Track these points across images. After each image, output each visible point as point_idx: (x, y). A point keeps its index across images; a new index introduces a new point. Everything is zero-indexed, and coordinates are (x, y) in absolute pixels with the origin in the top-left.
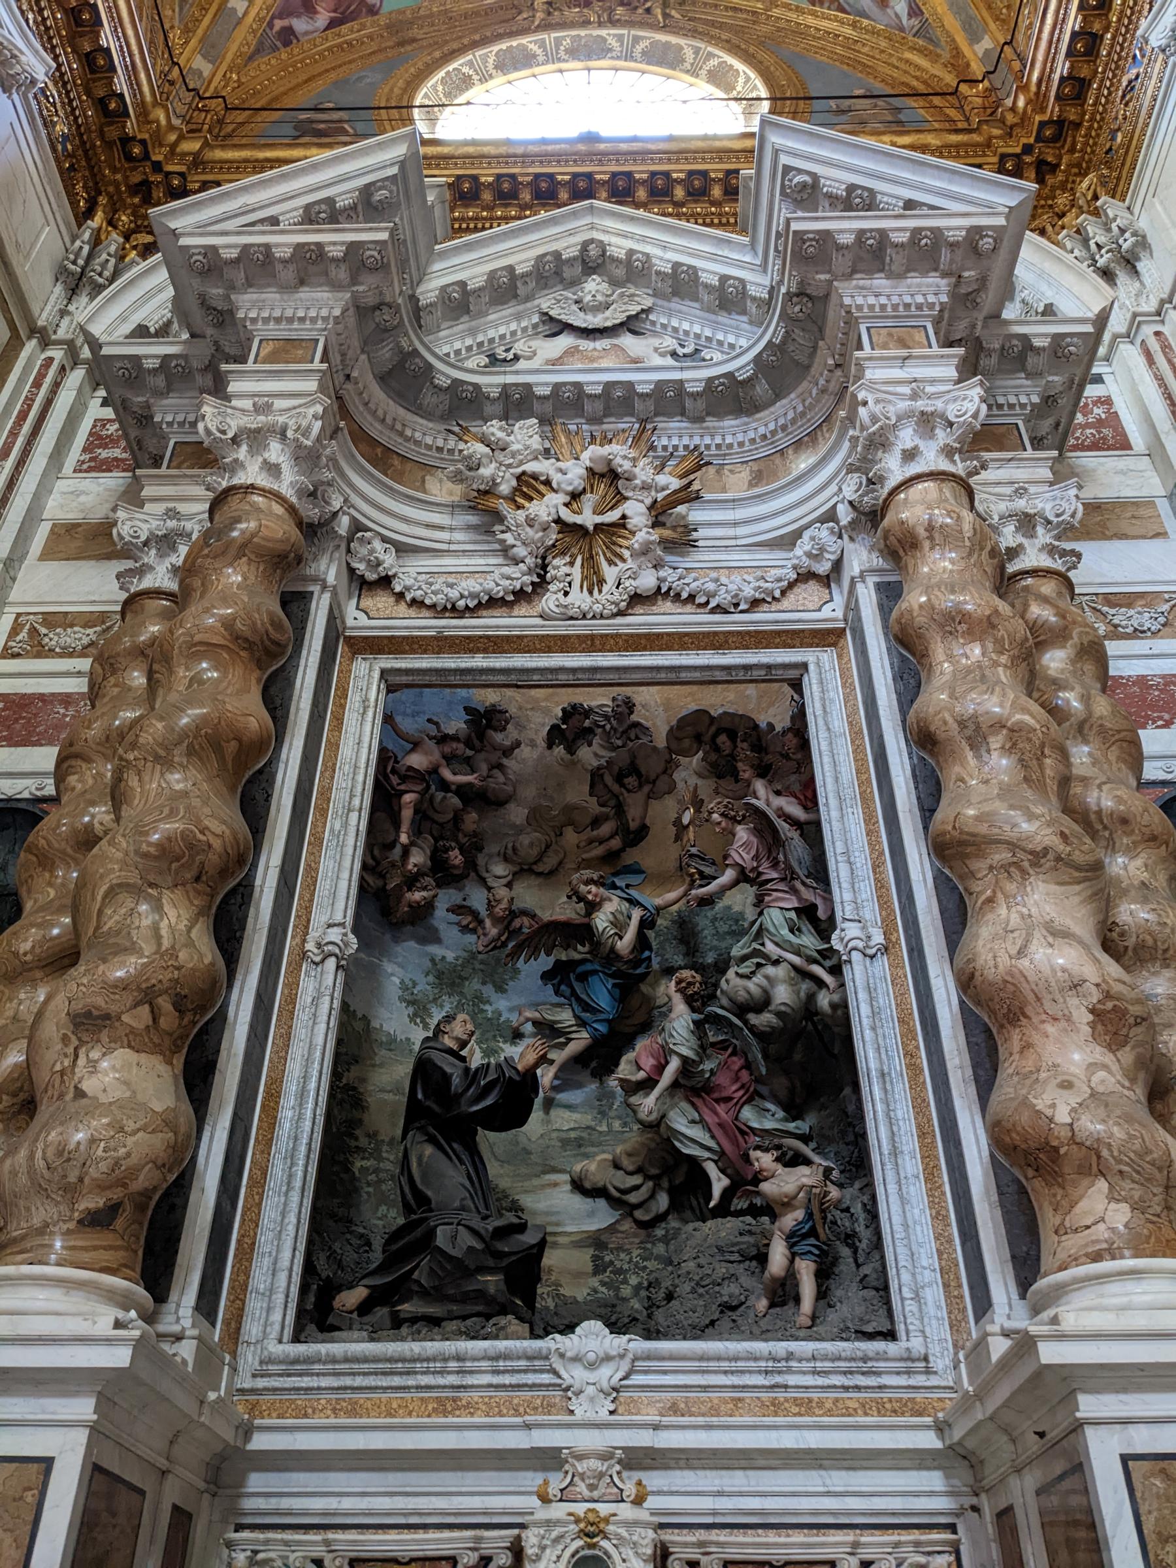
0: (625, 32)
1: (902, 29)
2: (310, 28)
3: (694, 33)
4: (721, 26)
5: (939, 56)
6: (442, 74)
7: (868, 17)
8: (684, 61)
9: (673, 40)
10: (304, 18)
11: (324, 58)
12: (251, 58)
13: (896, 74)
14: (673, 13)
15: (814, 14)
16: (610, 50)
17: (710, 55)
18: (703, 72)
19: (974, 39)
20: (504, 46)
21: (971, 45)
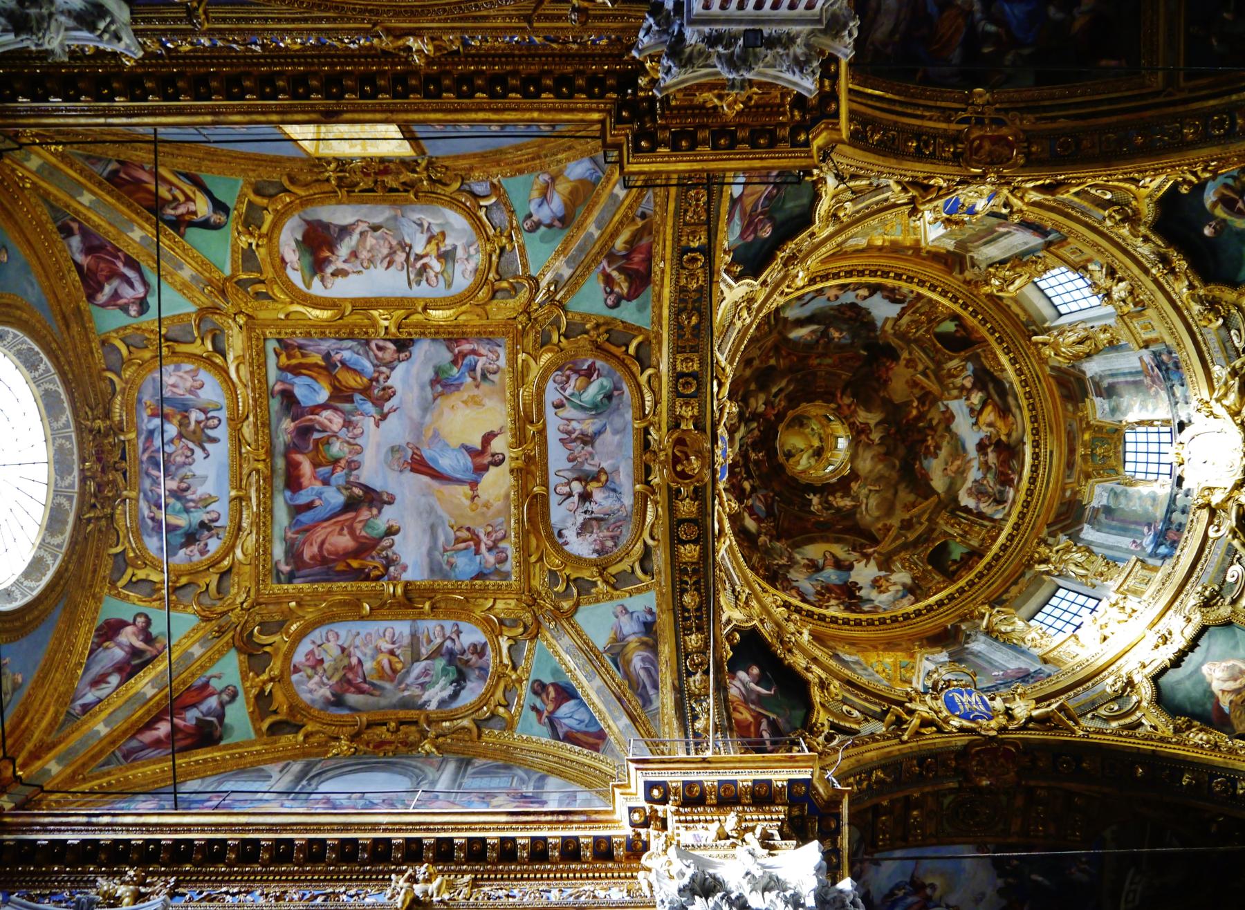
0: (76, 489)
1: (73, 701)
2: (74, 249)
3: (73, 542)
4: (80, 563)
5: (50, 734)
6: (37, 349)
7: (84, 673)
8: (52, 535)
9: (69, 528)
10: (81, 246)
11: (51, 257)
12: (46, 201)
13: (36, 704)
14: (91, 526)
15: (90, 631)
16: (62, 479)
17: (55, 557)
18: (42, 553)
19: (60, 759)
20: (63, 396)
21: (54, 757)
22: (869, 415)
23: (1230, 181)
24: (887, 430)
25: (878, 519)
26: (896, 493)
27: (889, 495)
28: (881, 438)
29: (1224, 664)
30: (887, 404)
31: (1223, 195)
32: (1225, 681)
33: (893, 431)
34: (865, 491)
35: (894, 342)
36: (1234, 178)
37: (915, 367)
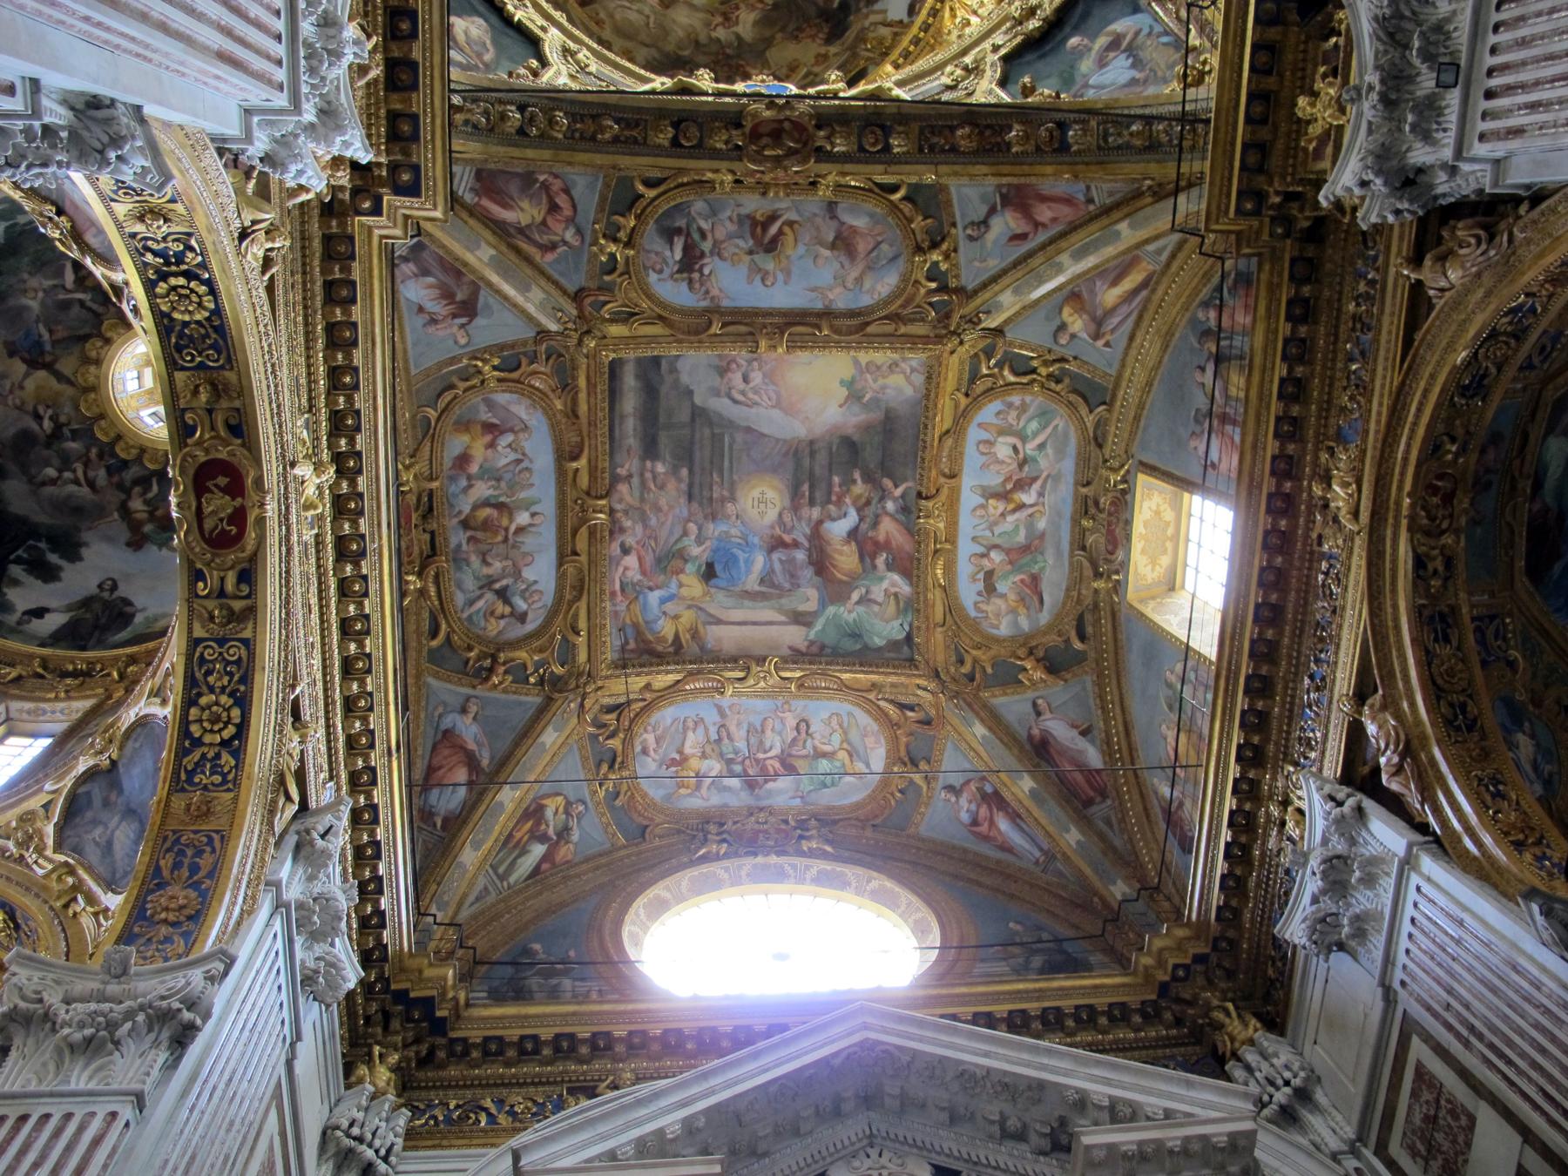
22: (749, 26)
23: (1145, 31)
24: (730, 45)
25: (611, 16)
26: (647, 46)
27: (643, 37)
28: (718, 40)
29: (488, 42)
30: (768, 42)
31: (1124, 36)
32: (466, 33)
33: (728, 51)
34: (647, 11)
35: (850, 35)
36: (1150, 34)
37: (817, 63)
